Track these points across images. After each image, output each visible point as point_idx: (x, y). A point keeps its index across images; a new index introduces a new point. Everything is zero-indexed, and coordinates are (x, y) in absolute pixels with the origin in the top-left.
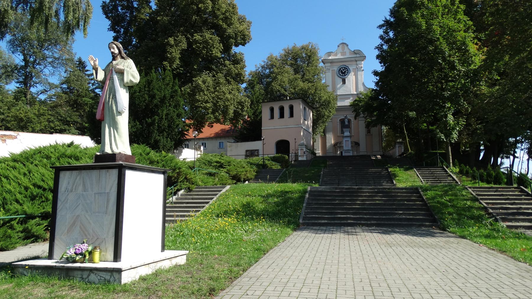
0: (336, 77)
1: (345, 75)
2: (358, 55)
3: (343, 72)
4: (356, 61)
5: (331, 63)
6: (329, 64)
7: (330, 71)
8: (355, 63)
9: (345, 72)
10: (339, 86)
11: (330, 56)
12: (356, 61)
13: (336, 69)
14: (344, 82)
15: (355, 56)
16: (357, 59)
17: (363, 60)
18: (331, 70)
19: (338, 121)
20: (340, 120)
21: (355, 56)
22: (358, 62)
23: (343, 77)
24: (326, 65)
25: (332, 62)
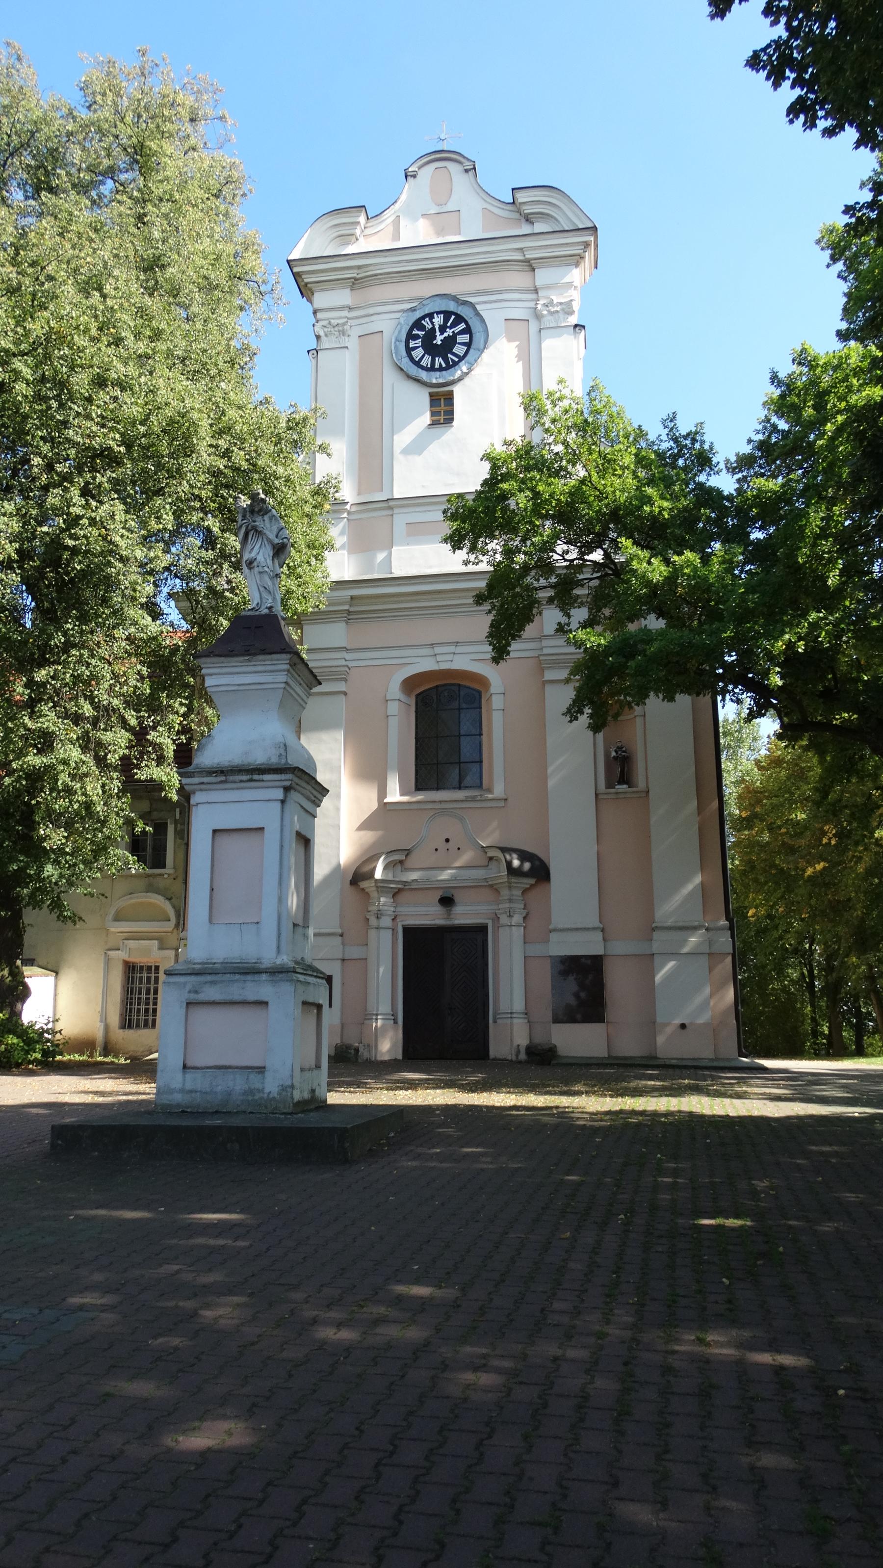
0: (390, 377)
1: (450, 366)
2: (539, 227)
3: (439, 344)
4: (530, 266)
5: (355, 284)
6: (343, 297)
7: (352, 342)
8: (518, 279)
9: (450, 342)
10: (403, 439)
11: (347, 238)
12: (530, 266)
13: (390, 325)
14: (442, 408)
15: (526, 229)
16: (534, 248)
17: (577, 260)
18: (355, 332)
19: (395, 689)
20: (409, 684)
21: (526, 229)
22: (543, 276)
23: (435, 378)
24: (321, 299)
25: (360, 277)
